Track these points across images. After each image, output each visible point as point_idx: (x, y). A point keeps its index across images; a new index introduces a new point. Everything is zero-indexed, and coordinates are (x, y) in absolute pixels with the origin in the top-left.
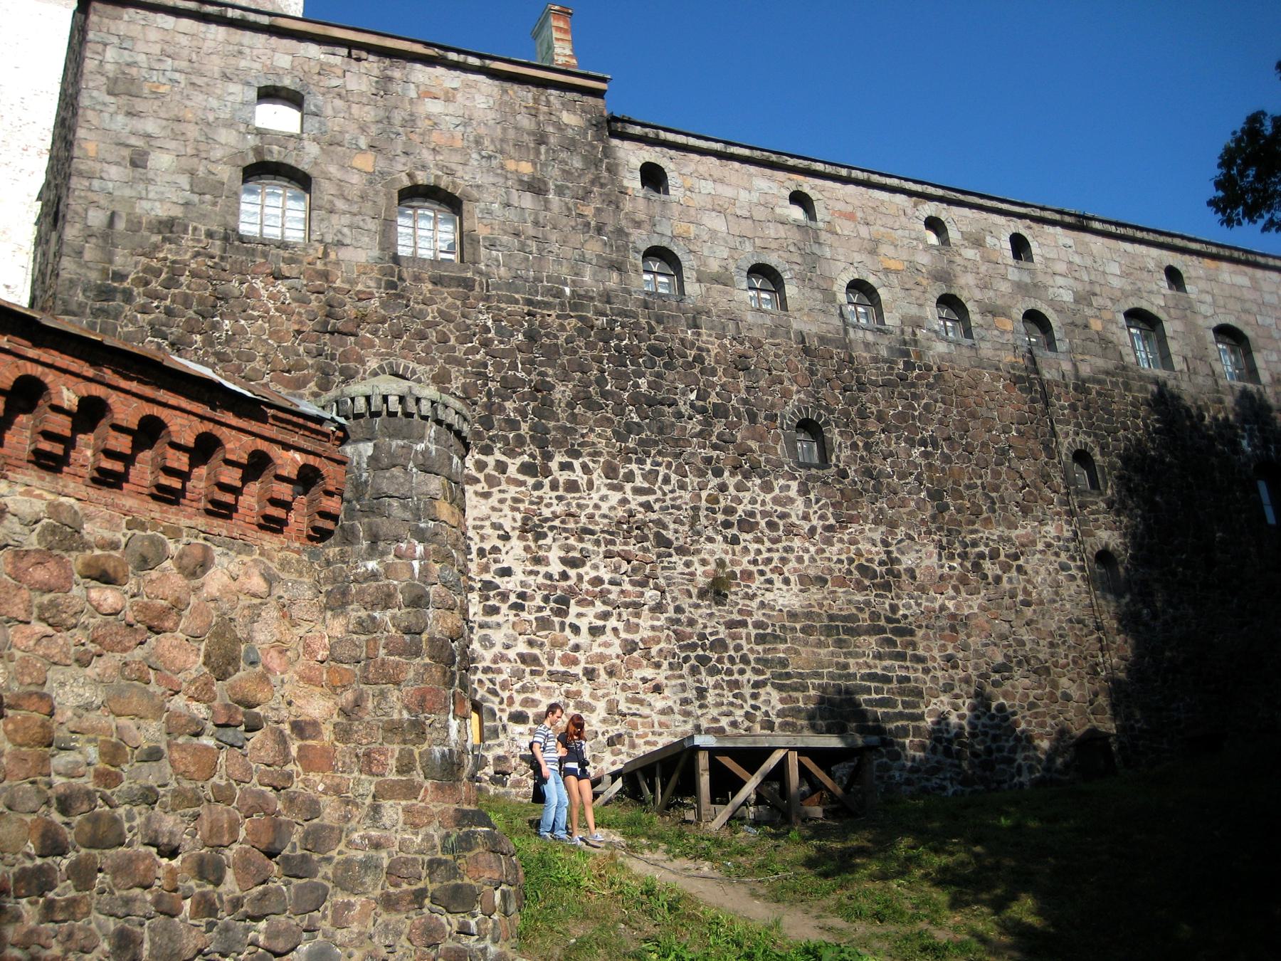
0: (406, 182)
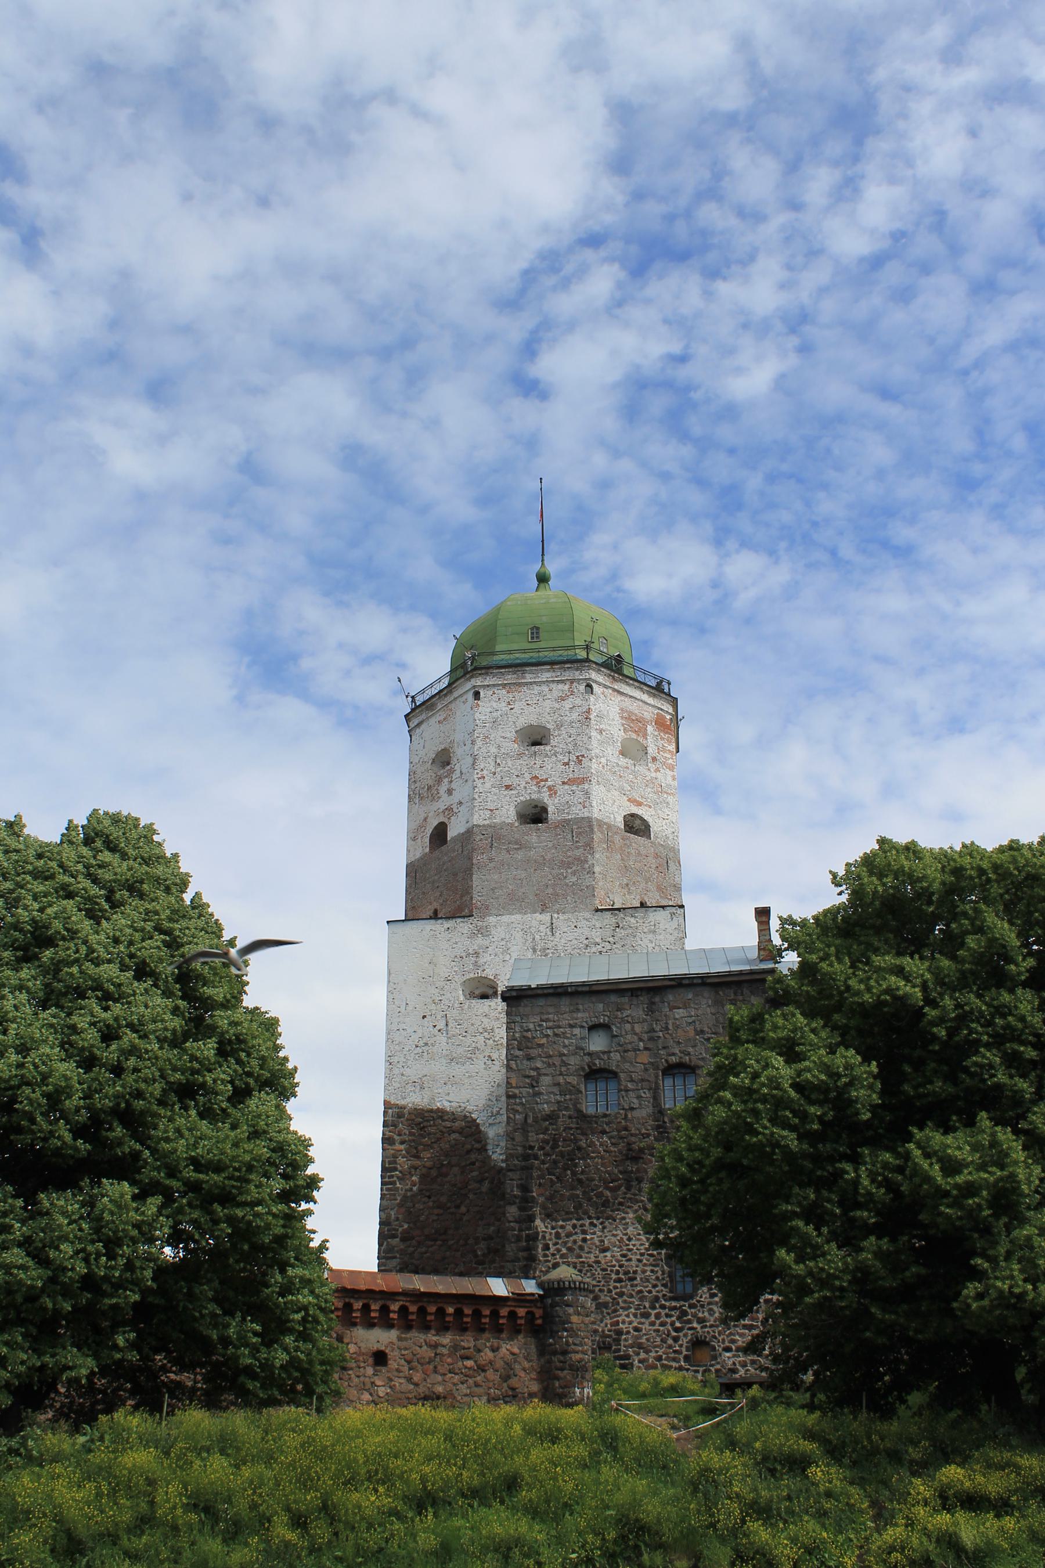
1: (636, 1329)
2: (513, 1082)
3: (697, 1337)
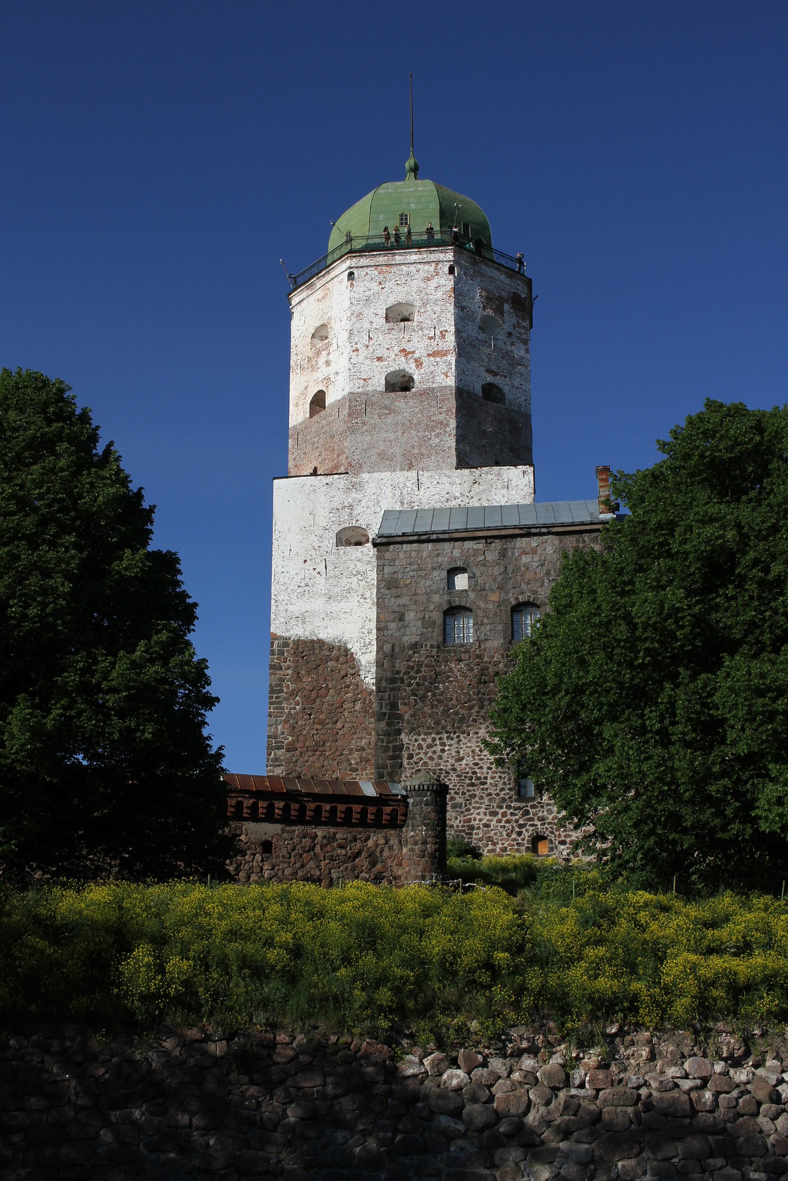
0: (514, 603)
1: (487, 826)
2: (382, 616)
3: (537, 832)
